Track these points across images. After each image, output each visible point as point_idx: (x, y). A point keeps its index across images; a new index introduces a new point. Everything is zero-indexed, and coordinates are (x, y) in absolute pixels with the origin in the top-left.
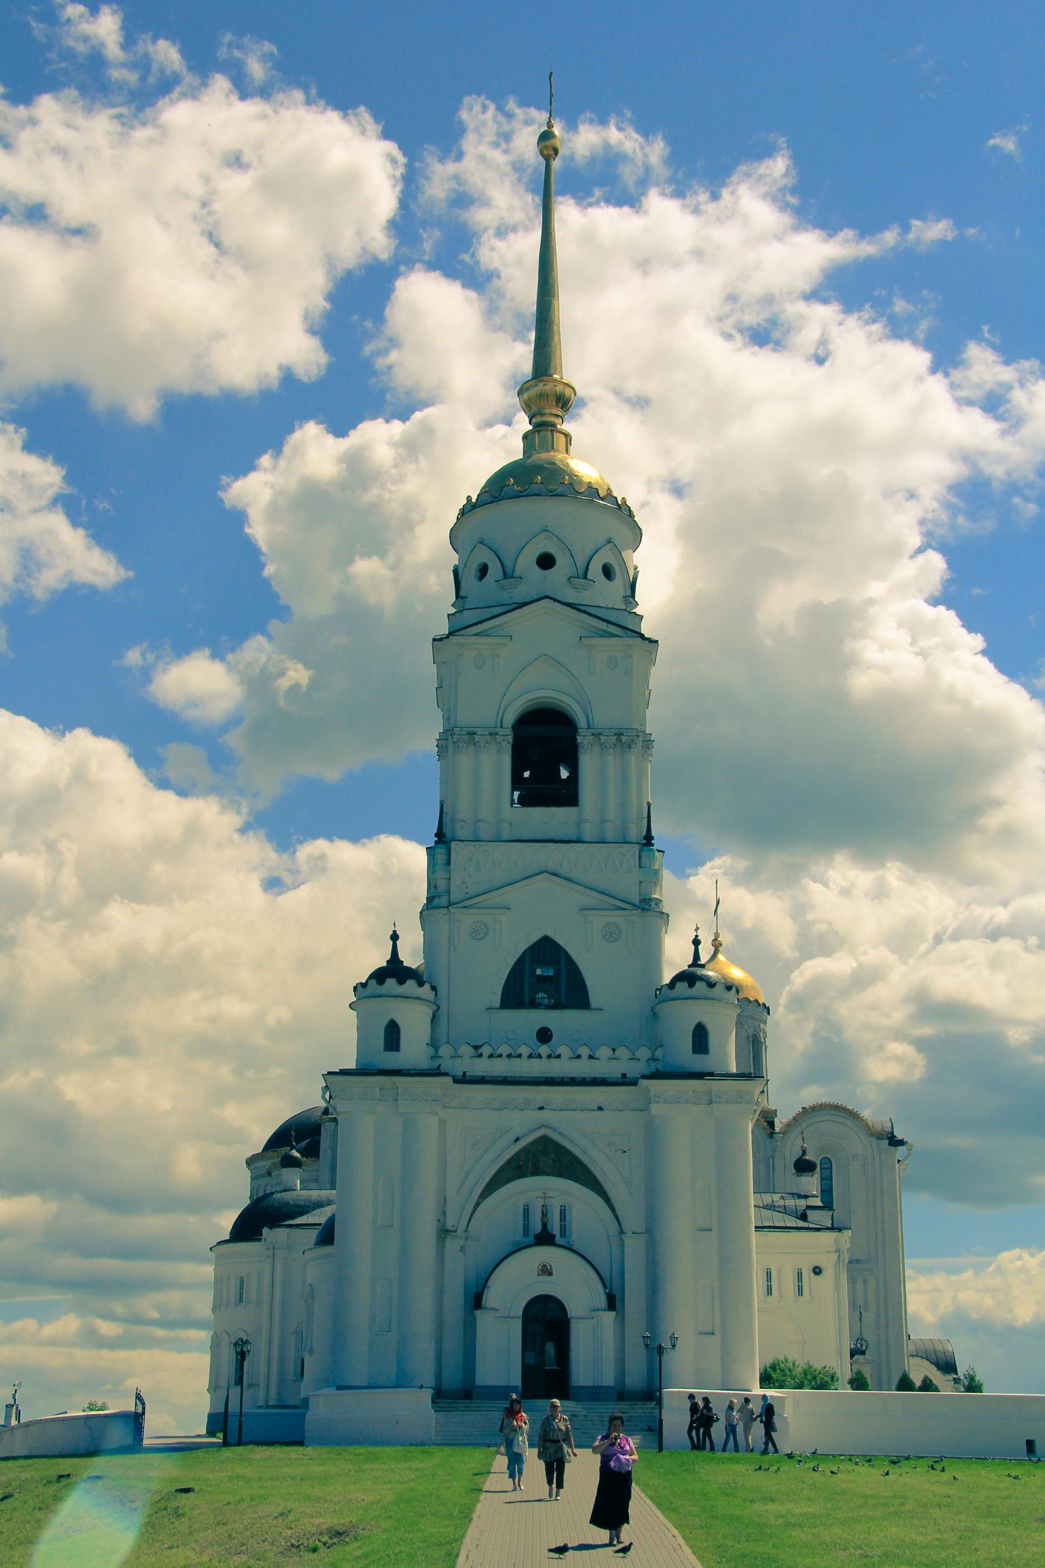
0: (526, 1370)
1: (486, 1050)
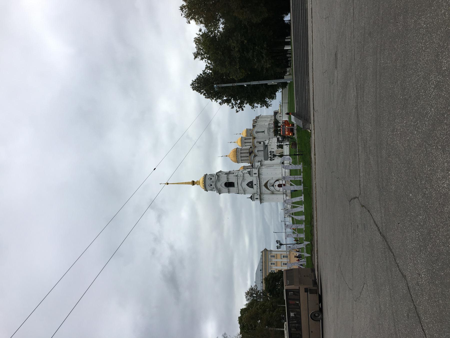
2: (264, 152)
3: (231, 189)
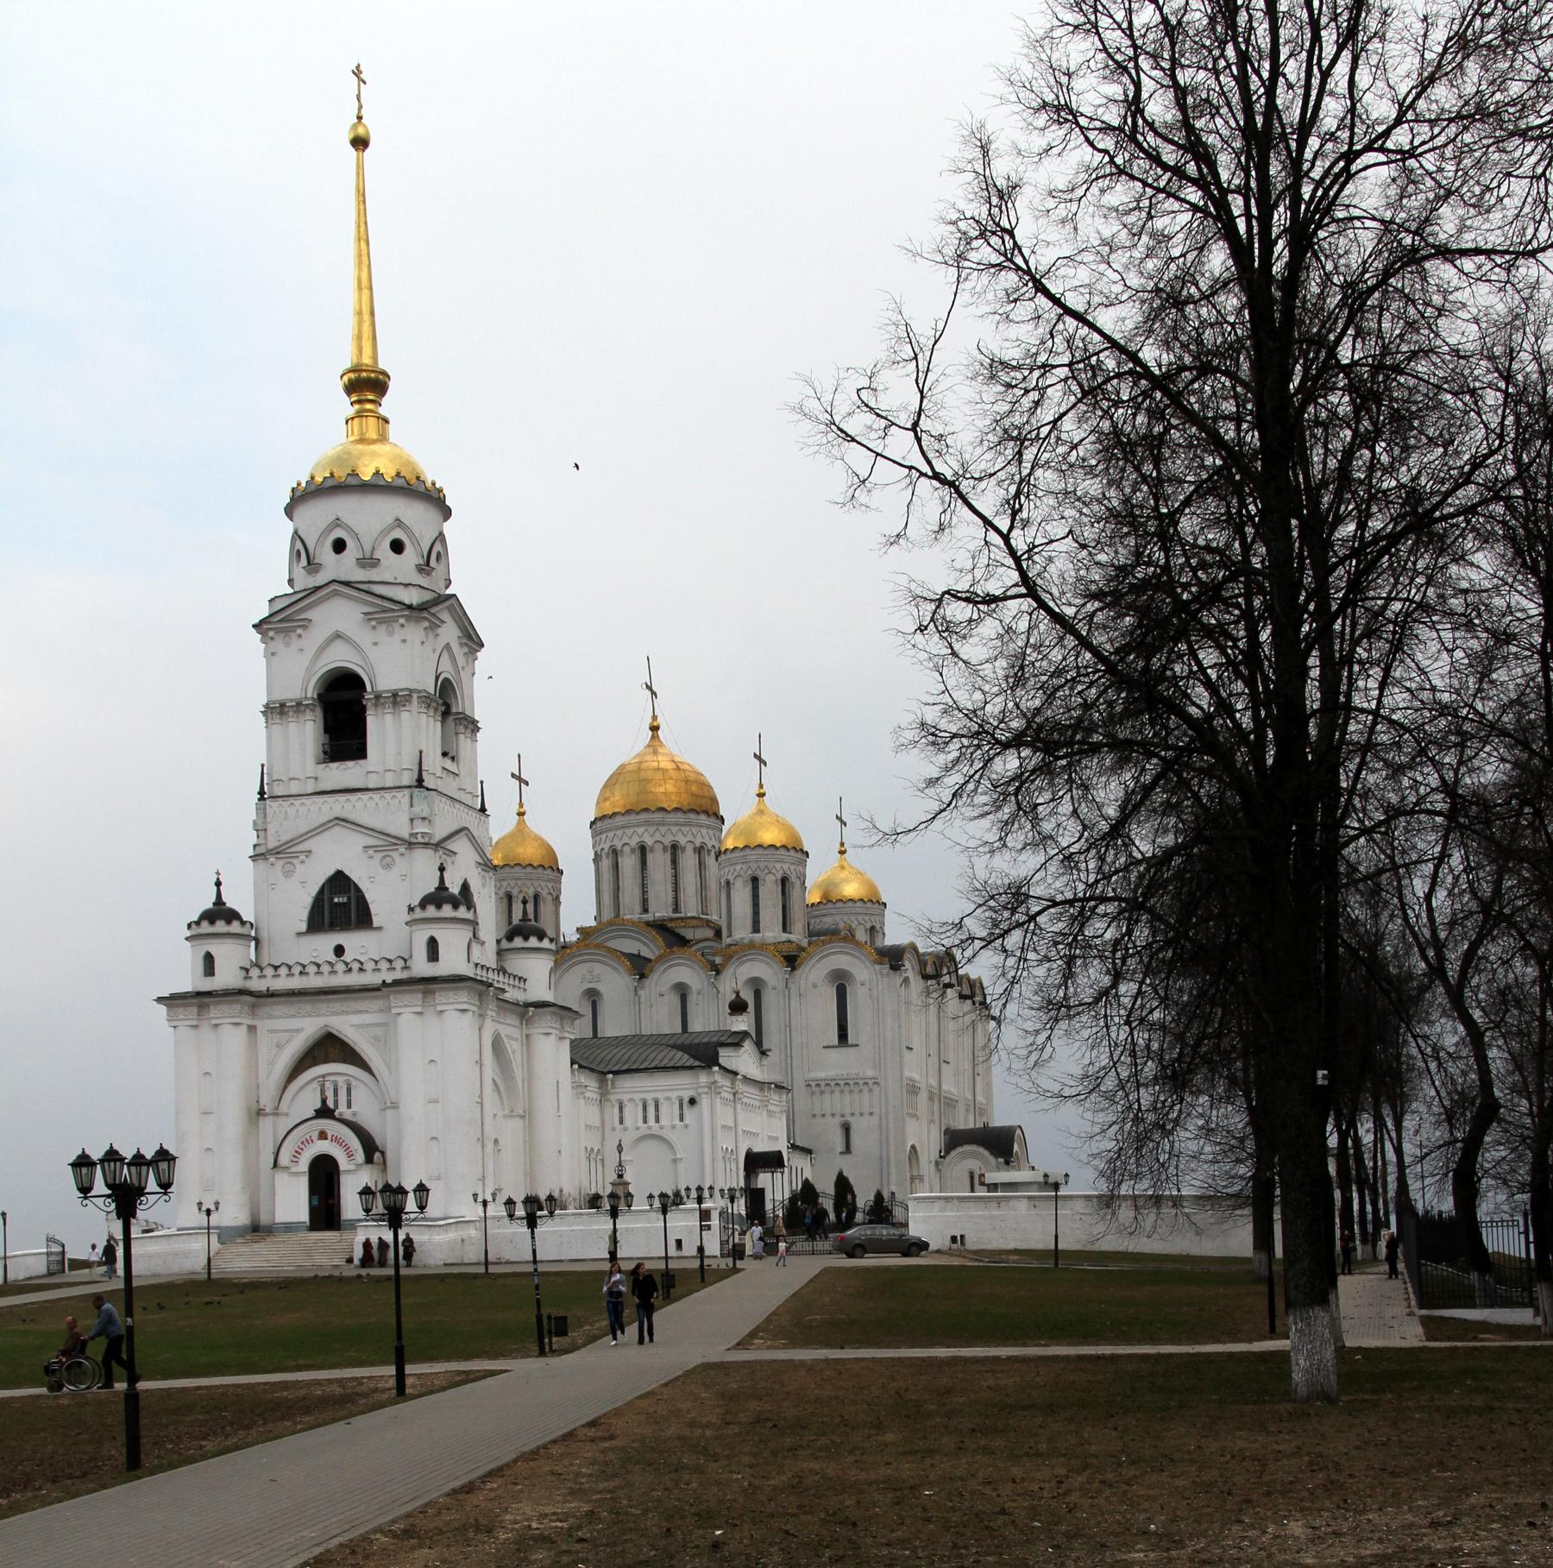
0: (313, 1211)
1: (283, 971)
2: (658, 1041)
3: (308, 732)
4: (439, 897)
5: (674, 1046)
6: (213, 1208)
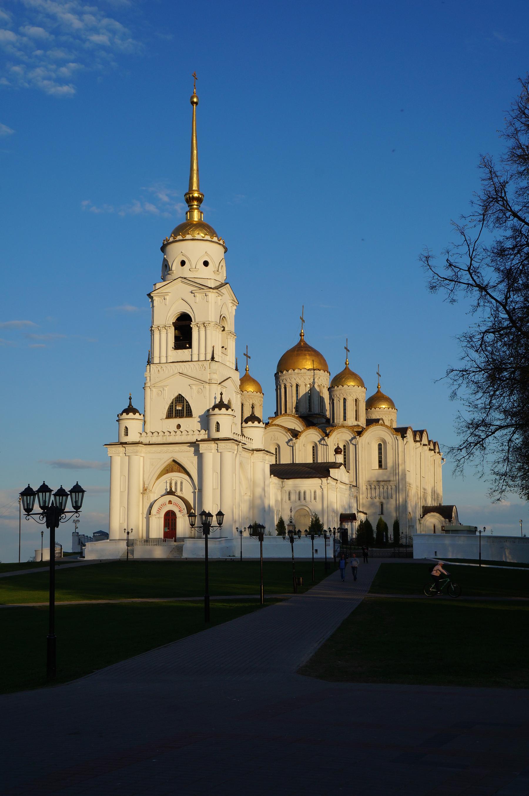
0: (165, 534)
1: (156, 434)
4: (221, 405)
5: (311, 468)
6: (130, 531)
